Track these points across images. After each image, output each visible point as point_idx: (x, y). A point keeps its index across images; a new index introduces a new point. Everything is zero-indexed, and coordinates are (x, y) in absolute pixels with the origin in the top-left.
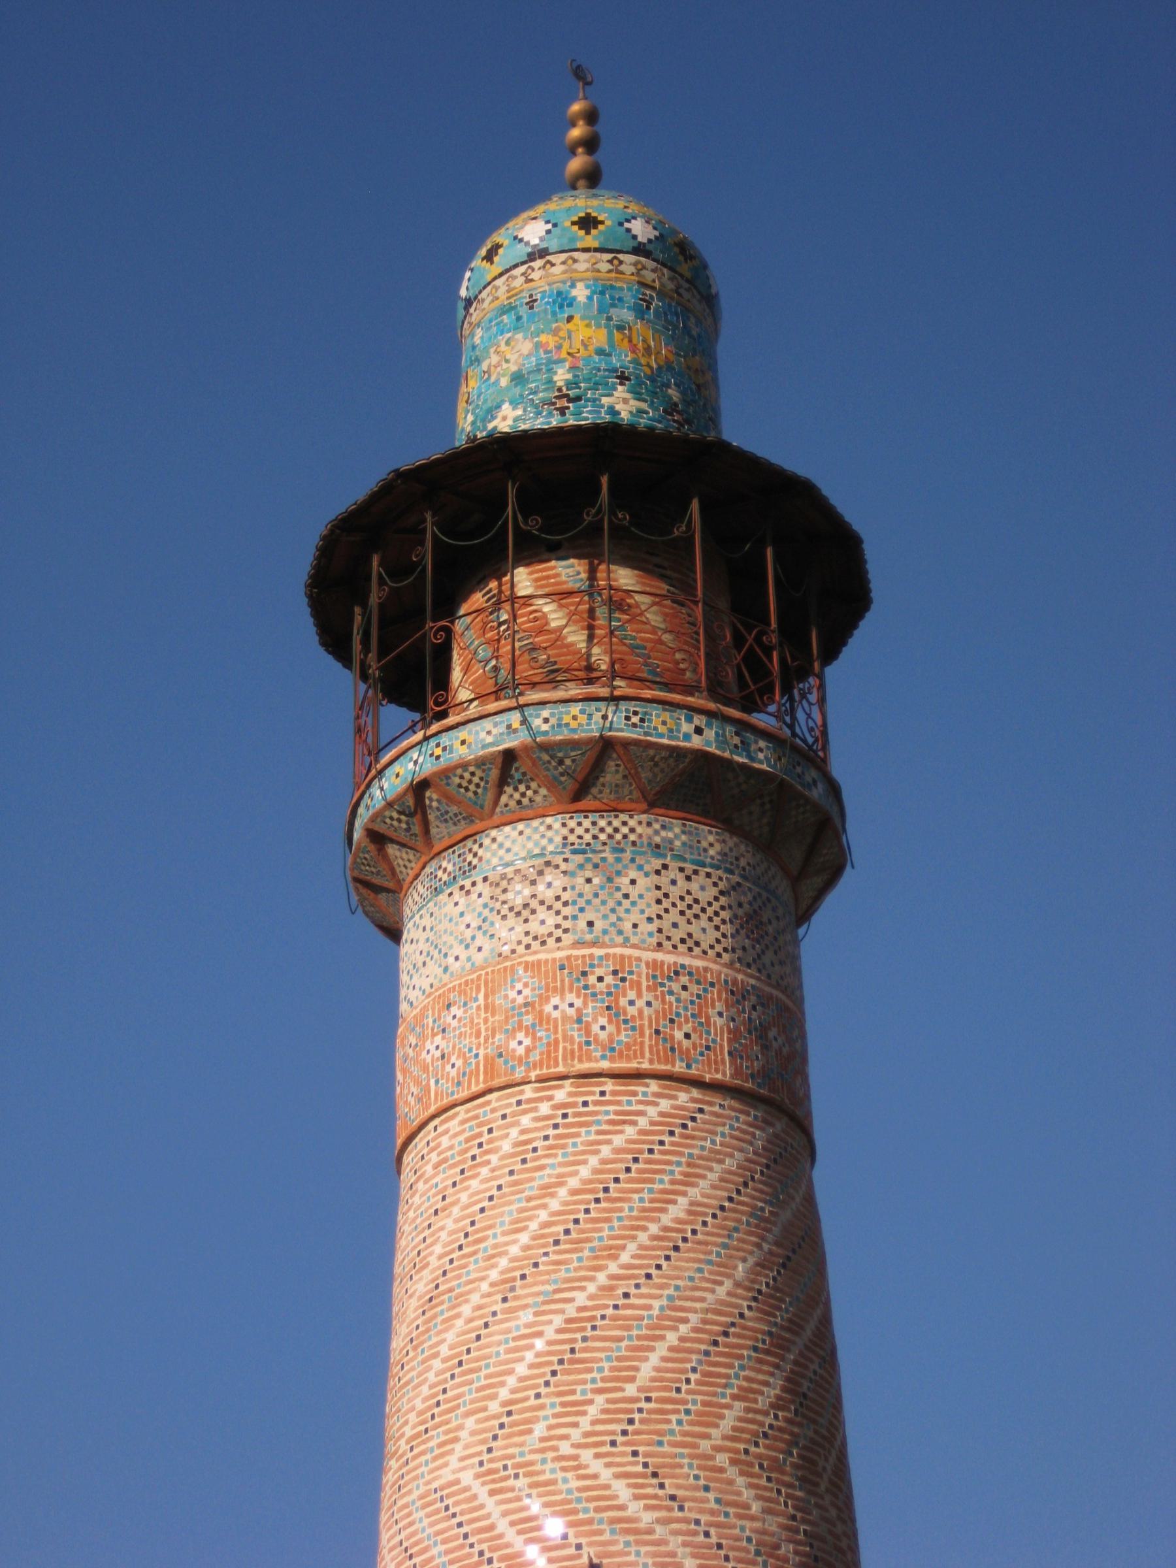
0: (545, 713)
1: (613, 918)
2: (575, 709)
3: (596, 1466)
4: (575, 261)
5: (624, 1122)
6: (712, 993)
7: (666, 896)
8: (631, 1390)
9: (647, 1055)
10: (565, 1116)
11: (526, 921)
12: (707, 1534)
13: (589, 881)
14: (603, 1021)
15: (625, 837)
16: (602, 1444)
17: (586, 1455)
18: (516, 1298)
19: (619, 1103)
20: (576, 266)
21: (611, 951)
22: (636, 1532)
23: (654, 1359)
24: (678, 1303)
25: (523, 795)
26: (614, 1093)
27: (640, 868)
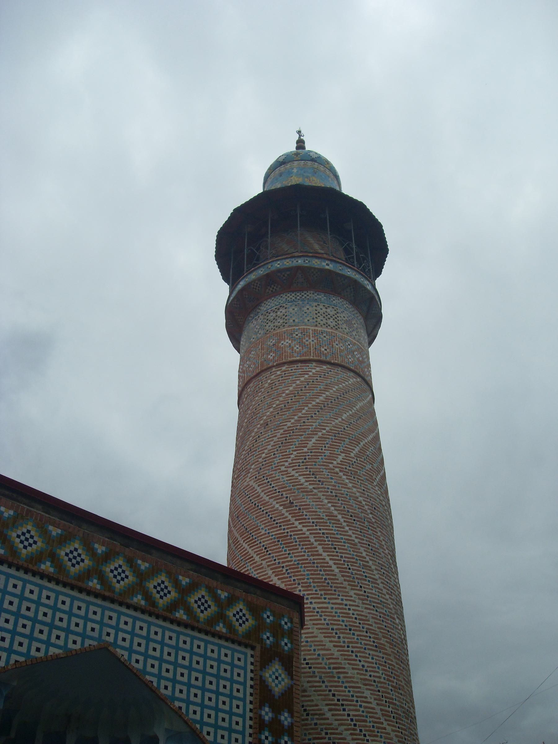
0: (279, 262)
1: (301, 319)
2: (288, 260)
3: (293, 473)
5: (305, 374)
7: (319, 312)
8: (305, 450)
9: (312, 355)
11: (274, 323)
12: (331, 492)
13: (294, 309)
14: (297, 346)
15: (305, 297)
16: (296, 466)
17: (290, 470)
18: (268, 427)
19: (303, 369)
20: (294, 165)
21: (301, 327)
22: (307, 492)
23: (313, 440)
25: (273, 288)
26: (301, 366)
27: (310, 305)
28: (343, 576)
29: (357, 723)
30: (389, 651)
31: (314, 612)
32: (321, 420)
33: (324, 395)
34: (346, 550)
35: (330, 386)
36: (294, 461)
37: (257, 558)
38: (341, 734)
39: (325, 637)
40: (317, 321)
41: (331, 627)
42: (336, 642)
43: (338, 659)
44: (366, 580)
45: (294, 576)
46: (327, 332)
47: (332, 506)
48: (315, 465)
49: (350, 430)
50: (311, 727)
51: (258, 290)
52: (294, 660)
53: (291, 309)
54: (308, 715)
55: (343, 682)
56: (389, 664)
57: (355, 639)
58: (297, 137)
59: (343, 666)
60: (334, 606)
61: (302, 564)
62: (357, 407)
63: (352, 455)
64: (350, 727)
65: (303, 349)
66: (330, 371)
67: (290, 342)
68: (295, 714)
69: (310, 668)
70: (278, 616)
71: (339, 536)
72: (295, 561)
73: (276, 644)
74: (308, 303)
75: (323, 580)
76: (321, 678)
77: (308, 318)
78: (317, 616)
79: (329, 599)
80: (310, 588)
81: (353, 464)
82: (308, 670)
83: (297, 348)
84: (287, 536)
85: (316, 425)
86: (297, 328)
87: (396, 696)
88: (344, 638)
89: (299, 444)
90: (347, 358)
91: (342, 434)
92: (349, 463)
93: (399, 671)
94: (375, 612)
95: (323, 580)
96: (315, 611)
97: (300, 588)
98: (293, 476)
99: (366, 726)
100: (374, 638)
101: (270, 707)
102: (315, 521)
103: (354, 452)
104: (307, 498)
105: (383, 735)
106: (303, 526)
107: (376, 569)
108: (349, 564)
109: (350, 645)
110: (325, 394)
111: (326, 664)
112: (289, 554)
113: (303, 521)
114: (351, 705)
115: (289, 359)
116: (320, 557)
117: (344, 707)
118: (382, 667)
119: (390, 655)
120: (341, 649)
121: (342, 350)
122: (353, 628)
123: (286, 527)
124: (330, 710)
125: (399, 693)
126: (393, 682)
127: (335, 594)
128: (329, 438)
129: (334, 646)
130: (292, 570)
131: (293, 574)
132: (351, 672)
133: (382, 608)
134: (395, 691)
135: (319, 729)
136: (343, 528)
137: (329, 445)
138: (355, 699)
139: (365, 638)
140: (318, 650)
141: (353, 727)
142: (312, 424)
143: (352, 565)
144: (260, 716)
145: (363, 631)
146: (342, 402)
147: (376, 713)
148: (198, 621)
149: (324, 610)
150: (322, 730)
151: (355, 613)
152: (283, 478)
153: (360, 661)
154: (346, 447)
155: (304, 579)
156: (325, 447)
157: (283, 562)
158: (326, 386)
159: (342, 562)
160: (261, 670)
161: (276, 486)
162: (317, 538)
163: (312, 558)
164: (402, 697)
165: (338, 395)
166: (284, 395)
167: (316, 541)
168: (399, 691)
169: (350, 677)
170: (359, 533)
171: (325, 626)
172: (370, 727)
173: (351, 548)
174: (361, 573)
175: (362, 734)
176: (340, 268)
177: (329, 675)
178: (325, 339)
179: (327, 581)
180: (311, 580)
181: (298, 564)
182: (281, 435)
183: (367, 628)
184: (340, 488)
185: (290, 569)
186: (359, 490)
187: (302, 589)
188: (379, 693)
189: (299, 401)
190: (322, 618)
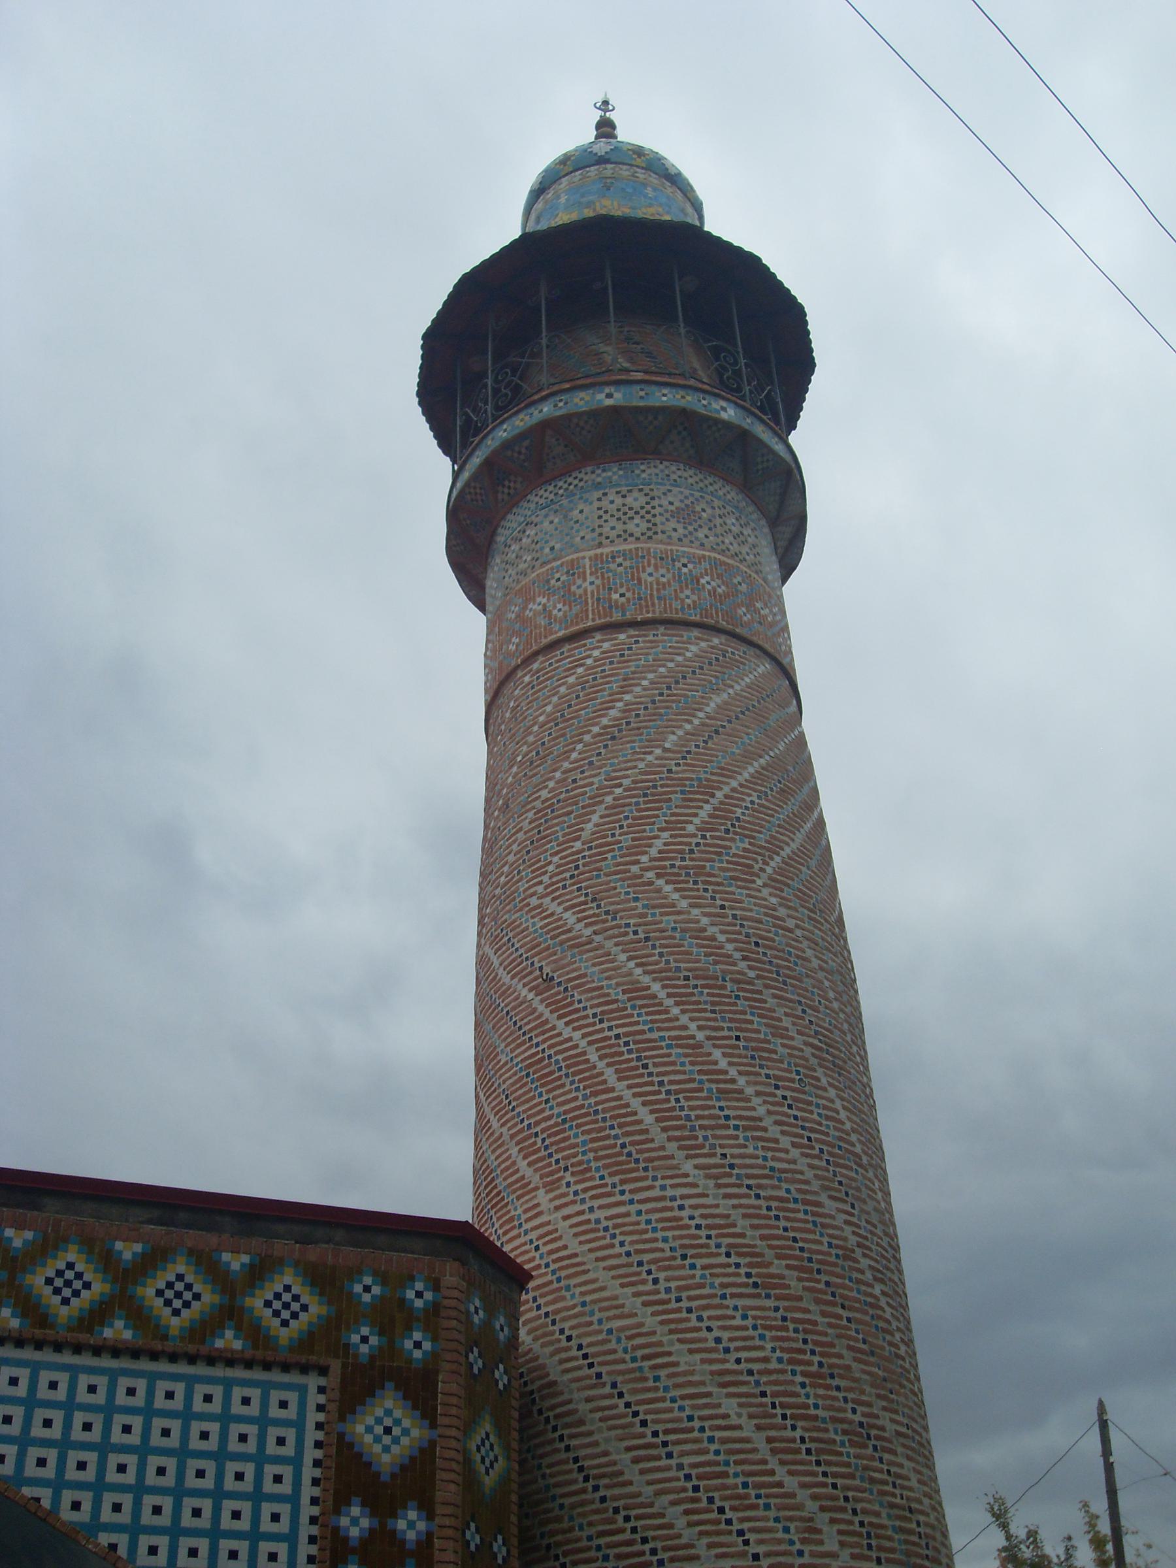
0: (505, 426)
2: (521, 416)
3: (554, 907)
6: (643, 562)
7: (606, 512)
8: (578, 845)
9: (590, 616)
10: (538, 678)
12: (636, 933)
15: (576, 486)
16: (557, 889)
23: (595, 818)
24: (613, 774)
25: (509, 488)
26: (570, 650)
27: (586, 501)
28: (665, 1129)
29: (702, 1483)
30: (796, 1287)
31: (599, 1230)
32: (612, 765)
33: (619, 704)
34: (673, 1063)
35: (633, 679)
36: (554, 879)
37: (495, 1124)
38: (663, 1515)
39: (623, 1286)
40: (600, 535)
41: (635, 1259)
42: (648, 1293)
43: (654, 1333)
44: (728, 1127)
45: (557, 1152)
46: (624, 554)
47: (637, 965)
48: (598, 876)
49: (684, 771)
50: (594, 1507)
52: (440, 1378)
53: (546, 524)
54: (586, 1479)
55: (666, 1389)
56: (794, 1320)
57: (698, 1277)
58: (597, 115)
59: (666, 1349)
60: (644, 1207)
61: (572, 1119)
62: (708, 709)
63: (691, 828)
64: (683, 1495)
65: (571, 609)
66: (637, 642)
67: (544, 601)
68: (440, 1509)
69: (591, 1366)
70: (394, 1280)
71: (655, 1035)
72: (559, 1115)
73: (390, 1350)
74: (581, 498)
75: (618, 1149)
76: (614, 1385)
77: (582, 534)
78: (604, 1238)
79: (631, 1192)
80: (588, 1175)
81: (691, 851)
82: (587, 1371)
83: (559, 609)
84: (543, 1059)
86: (559, 563)
87: (816, 1396)
88: (667, 1280)
90: (677, 598)
91: (662, 786)
92: (681, 852)
93: (830, 1331)
94: (753, 1201)
95: (618, 1149)
96: (601, 1227)
97: (568, 1178)
98: (552, 914)
99: (725, 1487)
100: (750, 1265)
101: (363, 1505)
102: (598, 1010)
103: (696, 820)
104: (581, 960)
105: (772, 1501)
106: (574, 1029)
107: (758, 1094)
108: (681, 1096)
109: (684, 1295)
110: (620, 700)
111: (625, 1351)
112: (547, 1101)
113: (575, 1016)
114: (686, 1441)
115: (544, 641)
116: (611, 1095)
117: (669, 1449)
118: (774, 1333)
119: (800, 1299)
120: (660, 1308)
121: (664, 585)
122: (690, 1252)
123: (540, 1039)
124: (636, 1460)
125: (828, 1387)
126: (810, 1363)
127: (646, 1178)
128: (630, 804)
129: (645, 1304)
130: (553, 1139)
131: (555, 1148)
132: (685, 1361)
133: (774, 1187)
134: (813, 1385)
135: (611, 1510)
136: (667, 1012)
137: (630, 821)
138: (696, 1424)
139: (723, 1270)
140: (609, 1319)
141: (690, 1494)
142: (591, 780)
143: (687, 1099)
144: (336, 1530)
145: (719, 1254)
146: (667, 708)
147: (754, 1450)
148: (165, 1337)
149: (619, 1221)
150: (616, 1510)
151: (697, 1213)
152: (534, 924)
153: (709, 1329)
154: (673, 815)
155: (575, 1155)
156: (621, 827)
157: (537, 1123)
158: (625, 680)
159: (663, 1096)
160: (342, 1419)
161: (521, 947)
162: (603, 1052)
163: (592, 1100)
164: (840, 1395)
165: (654, 695)
166: (536, 728)
167: (601, 1058)
168: (829, 1381)
169: (685, 1373)
170: (708, 1015)
171: (624, 1260)
172: (736, 1486)
173: (686, 1055)
174: (712, 1112)
175: (715, 1507)
176: (642, 393)
177: (632, 1376)
178: (621, 569)
179: (625, 1151)
180: (591, 1155)
181: (564, 1121)
182: (530, 823)
183: (729, 1245)
184: (658, 918)
185: (549, 1136)
186: (707, 910)
187: (572, 1180)
188: (764, 1400)
189: (563, 735)
190: (616, 1241)
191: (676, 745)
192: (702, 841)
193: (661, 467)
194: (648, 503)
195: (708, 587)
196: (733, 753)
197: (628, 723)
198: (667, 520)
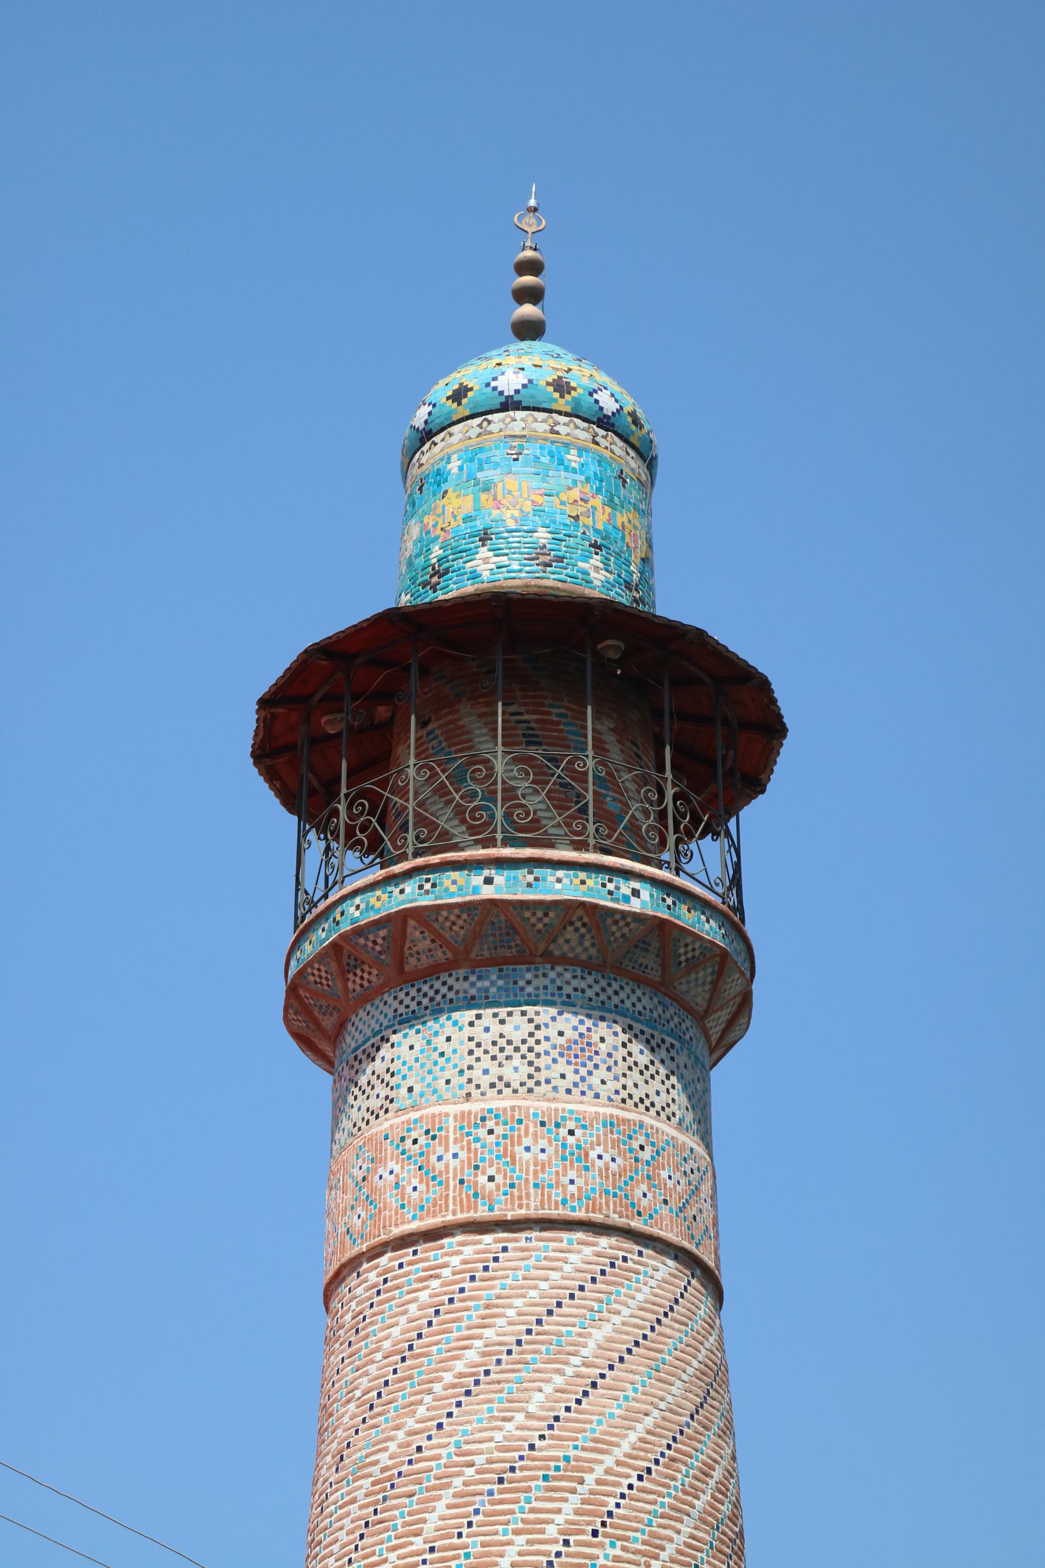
0: (357, 900)
4: (451, 435)
6: (519, 1130)
7: (479, 1045)
8: (418, 1543)
9: (451, 1206)
15: (444, 996)
23: (441, 1507)
24: (465, 1447)
25: (362, 978)
32: (465, 1433)
33: (478, 1343)
35: (497, 1306)
49: (550, 1447)
51: (328, 985)
62: (585, 1352)
65: (428, 1190)
66: (505, 1249)
77: (447, 1075)
85: (449, 1455)
89: (406, 1524)
91: (522, 1469)
103: (559, 1519)
110: (479, 1337)
137: (480, 1517)
154: (532, 1510)
156: (470, 1524)
166: (378, 1356)
176: (530, 878)
178: (491, 1138)
191: (542, 1408)
192: (563, 1549)
193: (552, 975)
194: (531, 1035)
195: (599, 1163)
196: (611, 1415)
197: (487, 1373)
198: (555, 1061)
